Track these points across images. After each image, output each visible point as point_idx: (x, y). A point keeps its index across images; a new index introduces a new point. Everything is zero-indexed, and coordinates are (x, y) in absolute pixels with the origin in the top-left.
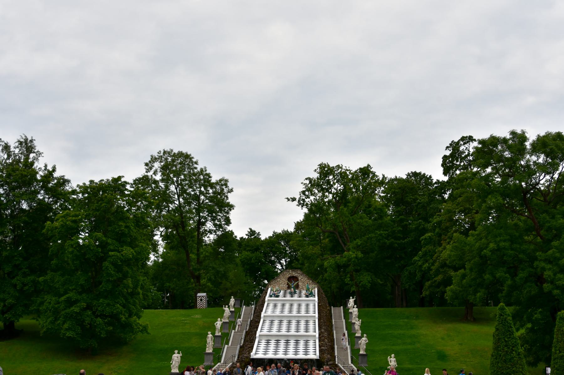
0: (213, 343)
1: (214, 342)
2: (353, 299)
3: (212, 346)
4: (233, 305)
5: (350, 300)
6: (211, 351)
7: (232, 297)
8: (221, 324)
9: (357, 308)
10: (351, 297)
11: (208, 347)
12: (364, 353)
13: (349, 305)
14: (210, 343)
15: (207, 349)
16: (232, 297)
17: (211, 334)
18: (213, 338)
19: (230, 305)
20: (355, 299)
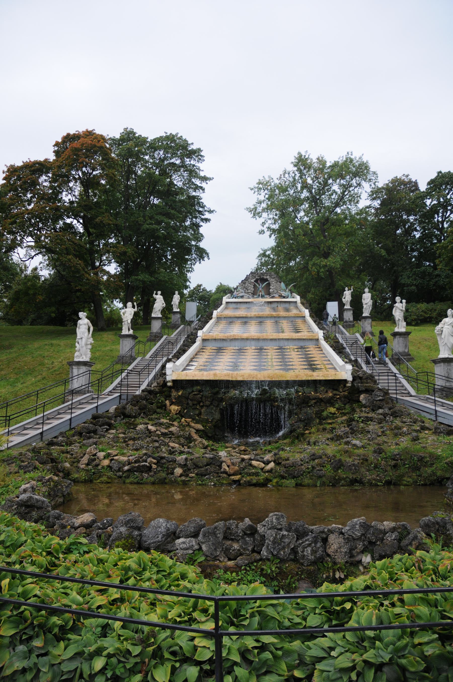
0: (91, 340)
1: (93, 336)
2: (350, 291)
3: (90, 347)
4: (177, 303)
5: (345, 292)
6: (86, 358)
7: (177, 292)
8: (133, 313)
9: (369, 292)
10: (346, 289)
11: (79, 351)
12: (450, 357)
13: (343, 300)
14: (84, 340)
15: (77, 354)
16: (177, 292)
17: (87, 317)
18: (92, 329)
19: (172, 303)
20: (352, 290)
